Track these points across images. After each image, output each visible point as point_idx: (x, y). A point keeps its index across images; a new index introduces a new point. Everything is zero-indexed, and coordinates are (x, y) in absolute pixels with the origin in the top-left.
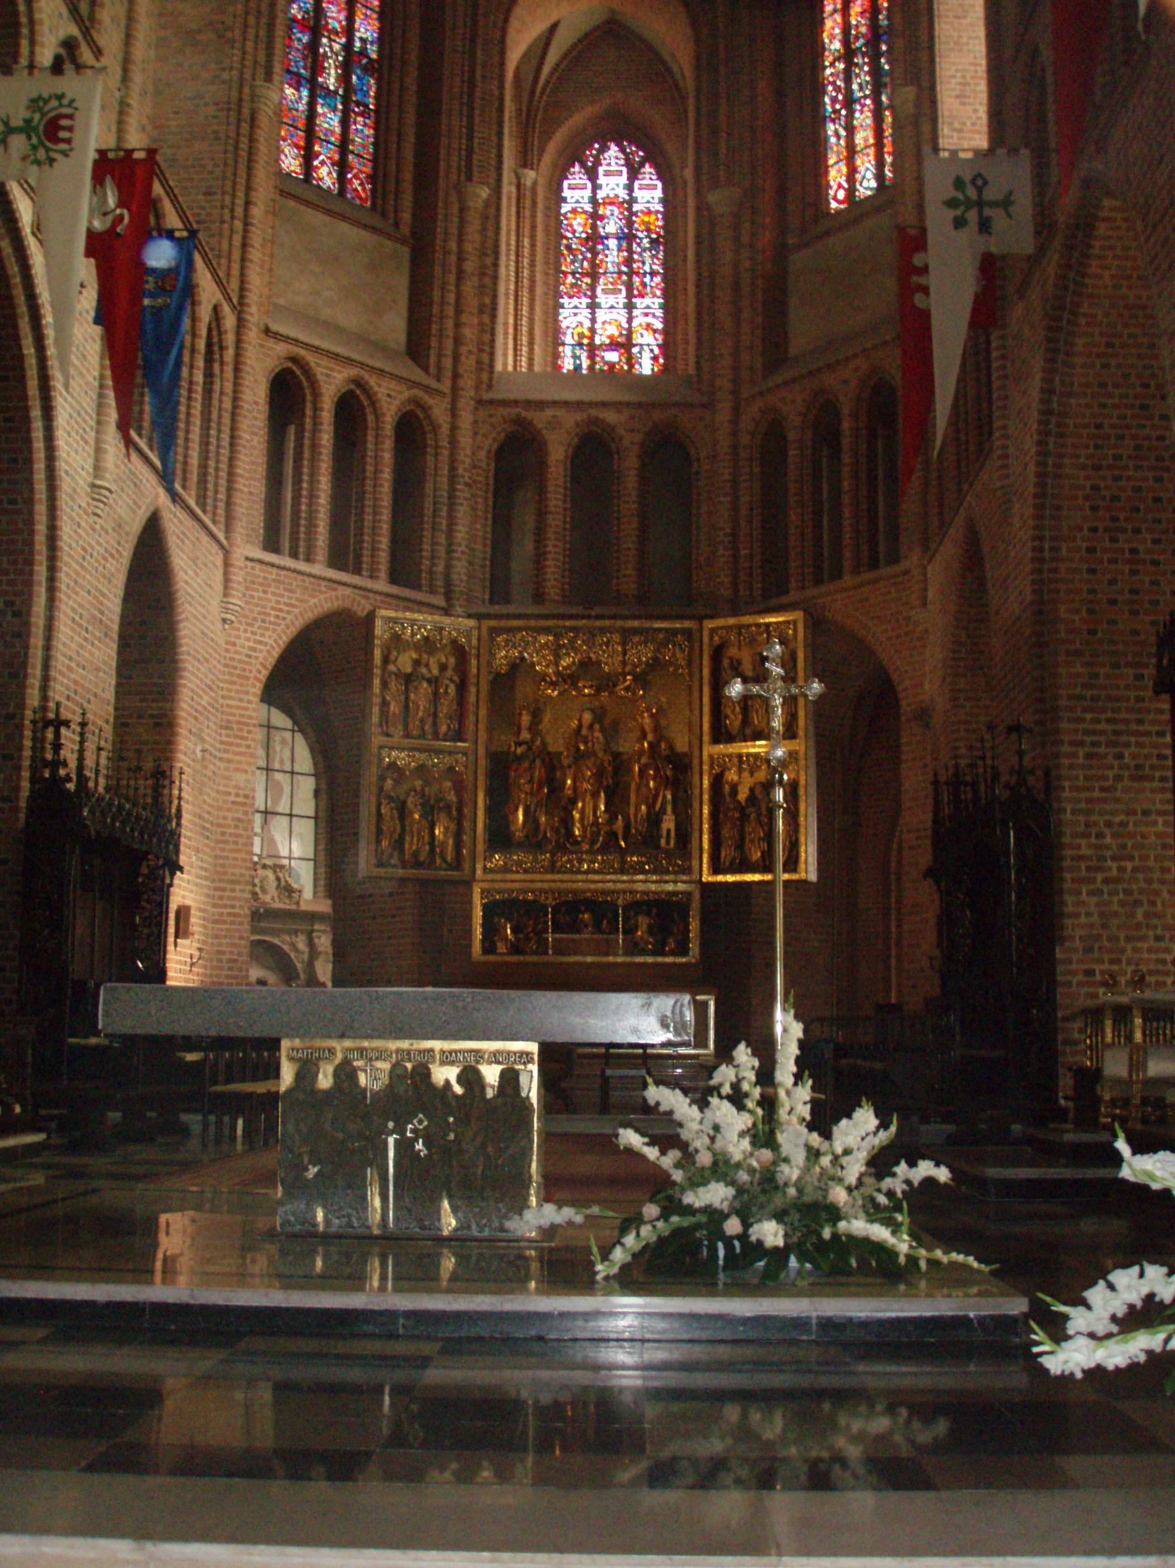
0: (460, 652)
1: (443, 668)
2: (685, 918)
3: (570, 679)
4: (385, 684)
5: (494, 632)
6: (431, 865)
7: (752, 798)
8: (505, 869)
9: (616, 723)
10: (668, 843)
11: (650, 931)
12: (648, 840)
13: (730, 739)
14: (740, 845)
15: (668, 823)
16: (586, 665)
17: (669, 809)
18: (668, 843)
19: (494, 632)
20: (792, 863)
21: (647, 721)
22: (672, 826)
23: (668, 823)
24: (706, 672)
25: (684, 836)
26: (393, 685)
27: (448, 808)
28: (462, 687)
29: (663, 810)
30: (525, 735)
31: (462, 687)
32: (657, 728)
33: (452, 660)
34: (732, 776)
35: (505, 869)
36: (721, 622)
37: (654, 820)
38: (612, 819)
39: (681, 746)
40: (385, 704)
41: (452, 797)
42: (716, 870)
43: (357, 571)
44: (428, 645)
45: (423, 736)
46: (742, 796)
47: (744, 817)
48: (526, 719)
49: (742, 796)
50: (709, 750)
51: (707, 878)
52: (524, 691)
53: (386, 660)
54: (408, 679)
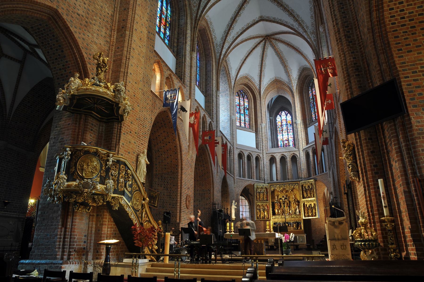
0: (266, 189)
2: (301, 224)
3: (282, 191)
6: (265, 218)
7: (309, 206)
8: (275, 218)
9: (289, 197)
11: (296, 226)
12: (295, 213)
13: (305, 198)
14: (308, 213)
15: (298, 210)
16: (284, 189)
19: (271, 185)
21: (293, 196)
23: (298, 210)
25: (300, 212)
28: (267, 193)
30: (276, 199)
31: (267, 193)
32: (295, 197)
34: (306, 203)
35: (275, 218)
37: (296, 210)
38: (290, 211)
39: (299, 199)
42: (305, 217)
43: (252, 179)
44: (262, 188)
46: (308, 206)
47: (308, 209)
48: (276, 197)
49: (308, 206)
50: (303, 200)
51: (304, 218)
52: (276, 193)
53: (256, 190)
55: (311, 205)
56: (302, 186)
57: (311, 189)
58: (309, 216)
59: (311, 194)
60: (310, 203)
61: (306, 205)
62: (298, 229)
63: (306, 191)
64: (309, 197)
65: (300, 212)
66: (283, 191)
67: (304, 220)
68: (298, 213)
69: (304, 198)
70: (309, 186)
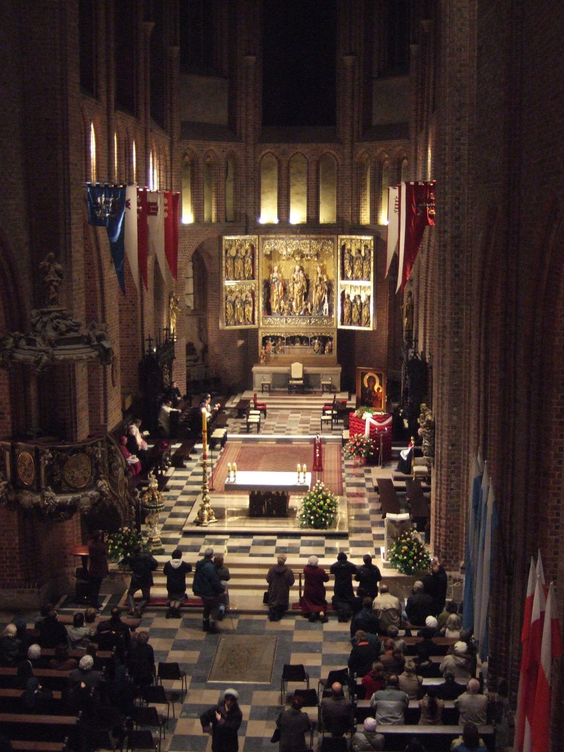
1: (247, 252)
4: (226, 261)
5: (264, 239)
7: (355, 301)
10: (326, 313)
13: (347, 279)
15: (326, 306)
17: (326, 301)
18: (326, 313)
20: (367, 323)
22: (327, 308)
23: (326, 306)
24: (339, 254)
25: (331, 311)
26: (229, 262)
27: (249, 303)
29: (324, 302)
33: (249, 251)
36: (344, 237)
37: (321, 304)
38: (306, 304)
39: (331, 276)
40: (226, 268)
41: (250, 299)
45: (240, 279)
46: (352, 298)
49: (352, 298)
50: (341, 282)
54: (234, 258)
55: (360, 297)
56: (343, 248)
57: (364, 258)
58: (351, 323)
59: (362, 270)
60: (358, 292)
61: (349, 296)
62: (323, 352)
63: (352, 259)
64: (357, 278)
65: (331, 311)
66: (293, 256)
67: (340, 331)
68: (325, 313)
69: (344, 277)
70: (360, 251)
